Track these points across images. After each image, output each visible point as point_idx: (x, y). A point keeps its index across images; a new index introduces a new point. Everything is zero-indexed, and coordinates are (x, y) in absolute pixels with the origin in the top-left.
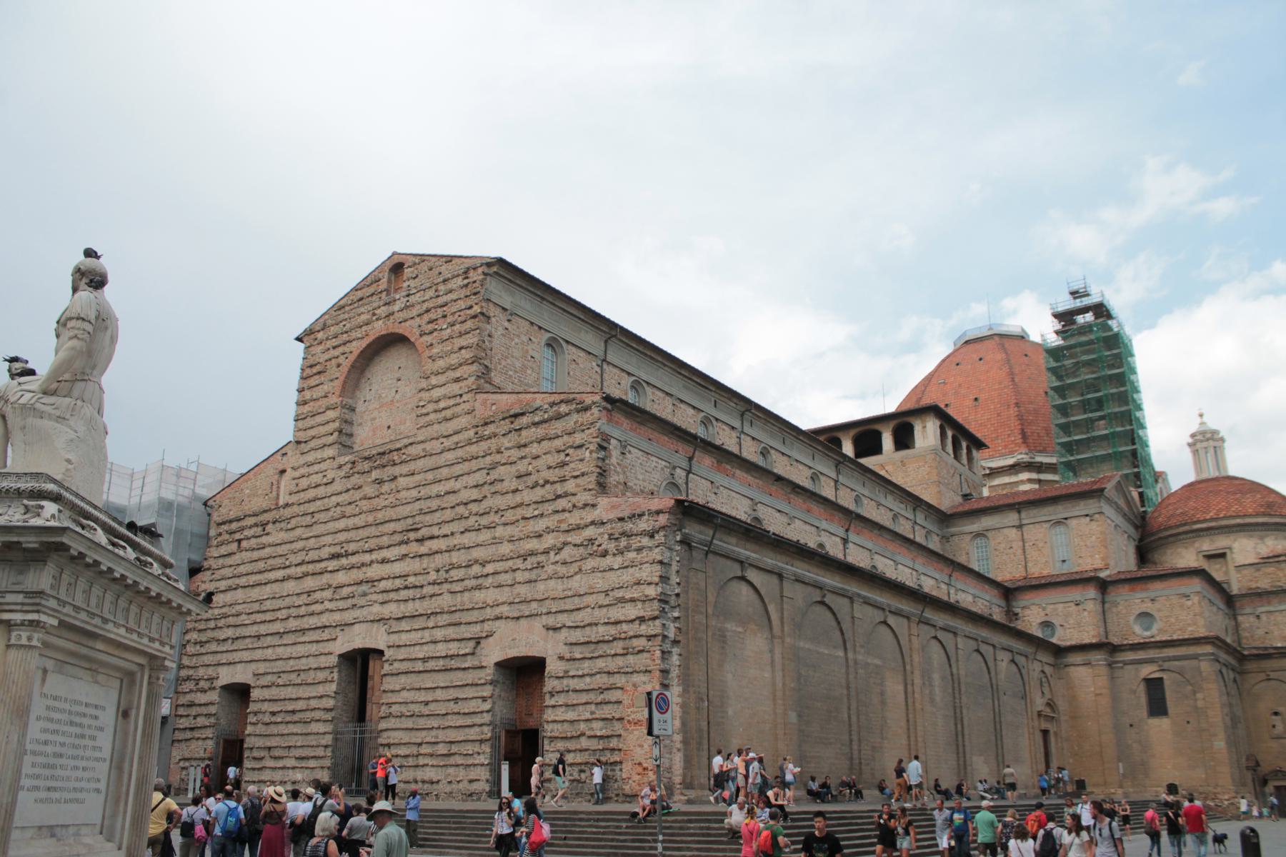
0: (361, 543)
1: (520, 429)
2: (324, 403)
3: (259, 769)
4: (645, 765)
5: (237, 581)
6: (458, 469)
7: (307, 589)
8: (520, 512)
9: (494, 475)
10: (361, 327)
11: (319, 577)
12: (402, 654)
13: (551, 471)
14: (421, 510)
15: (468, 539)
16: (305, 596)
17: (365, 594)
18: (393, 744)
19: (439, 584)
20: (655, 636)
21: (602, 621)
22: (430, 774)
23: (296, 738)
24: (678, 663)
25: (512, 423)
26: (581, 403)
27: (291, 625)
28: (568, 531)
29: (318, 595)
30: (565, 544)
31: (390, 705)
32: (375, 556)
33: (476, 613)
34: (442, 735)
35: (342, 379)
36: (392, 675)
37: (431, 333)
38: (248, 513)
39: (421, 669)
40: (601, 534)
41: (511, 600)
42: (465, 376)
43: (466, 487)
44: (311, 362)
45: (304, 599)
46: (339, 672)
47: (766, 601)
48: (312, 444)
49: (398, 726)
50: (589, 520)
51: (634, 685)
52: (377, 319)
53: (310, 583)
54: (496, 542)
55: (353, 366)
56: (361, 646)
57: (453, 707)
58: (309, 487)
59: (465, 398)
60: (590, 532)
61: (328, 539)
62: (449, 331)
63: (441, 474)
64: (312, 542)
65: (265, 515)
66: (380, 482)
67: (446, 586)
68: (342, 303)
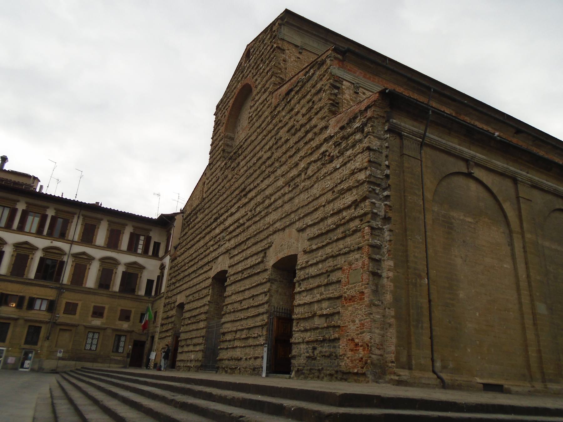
4: (357, 341)
9: (278, 137)
20: (365, 214)
22: (238, 353)
24: (388, 238)
30: (309, 164)
46: (213, 289)
47: (500, 199)
51: (350, 264)
54: (276, 180)
55: (230, 114)
57: (251, 302)
66: (233, 169)
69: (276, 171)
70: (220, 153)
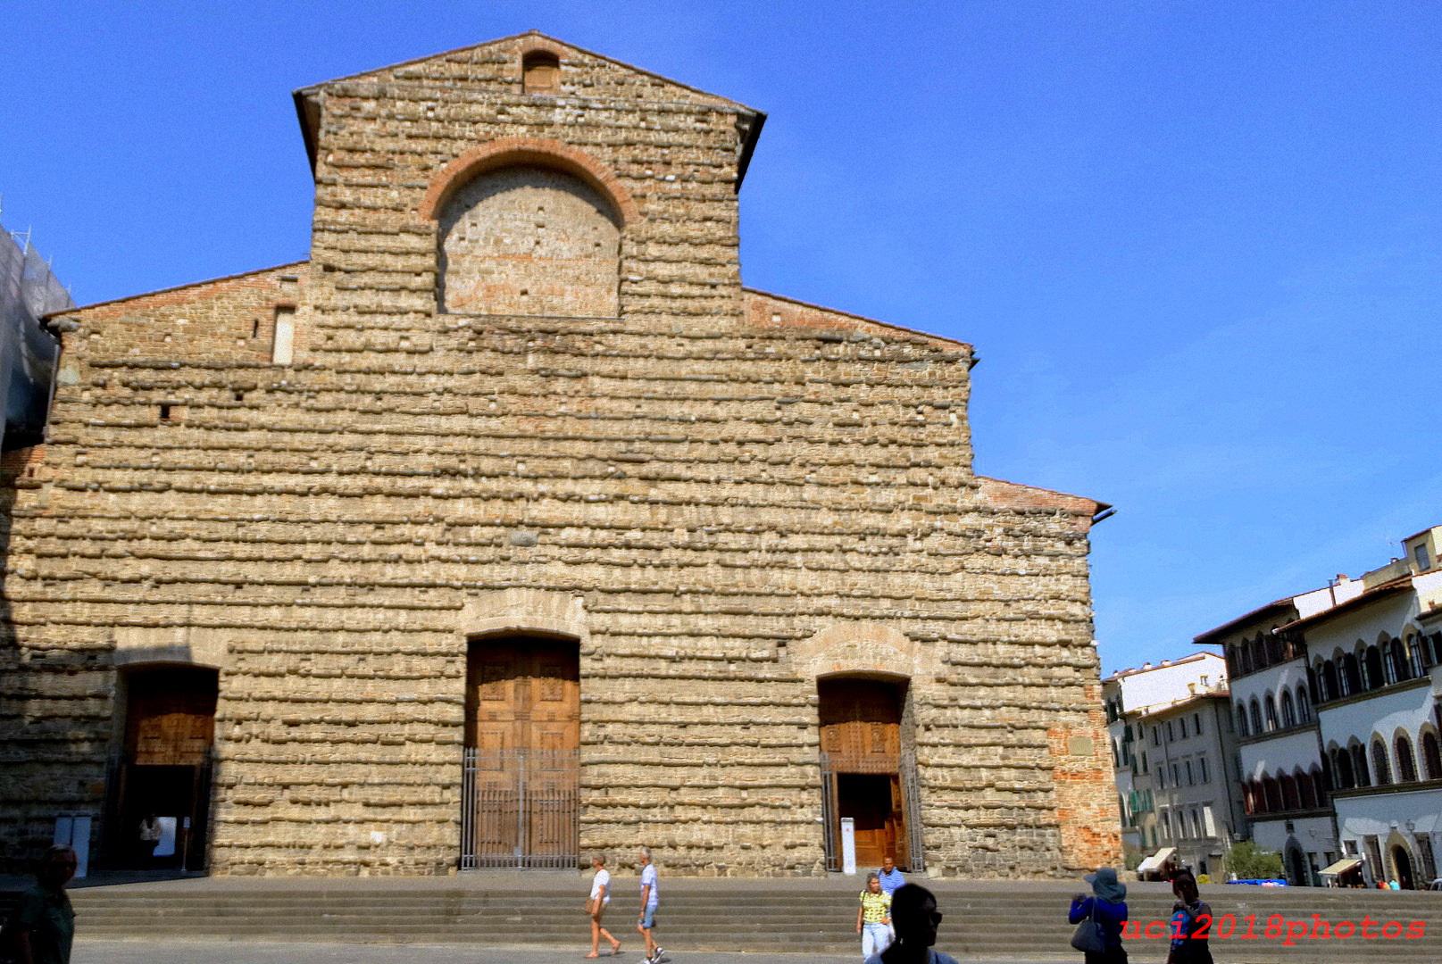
0: (506, 462)
1: (836, 360)
2: (393, 221)
3: (265, 823)
5: (163, 477)
6: (719, 390)
7: (379, 518)
8: (844, 474)
9: (793, 412)
10: (475, 123)
11: (405, 502)
12: (623, 645)
13: (896, 428)
14: (649, 434)
15: (746, 492)
16: (371, 527)
17: (528, 544)
18: (612, 787)
19: (695, 550)
21: (1006, 639)
23: (362, 768)
25: (818, 348)
26: (937, 351)
27: (332, 573)
28: (935, 513)
29: (406, 530)
30: (934, 530)
31: (601, 723)
32: (544, 487)
33: (775, 600)
34: (722, 776)
35: (439, 190)
36: (603, 677)
37: (642, 178)
38: (187, 360)
39: (672, 672)
40: (991, 527)
41: (846, 590)
42: (724, 261)
43: (738, 419)
44: (350, 144)
45: (368, 531)
48: (366, 279)
49: (629, 757)
50: (968, 504)
52: (514, 123)
53: (379, 507)
56: (524, 625)
58: (368, 347)
59: (722, 291)
60: (970, 520)
61: (428, 443)
62: (677, 186)
63: (683, 389)
64: (381, 441)
65: (241, 372)
66: (550, 375)
67: (711, 556)
68: (412, 68)
69: (801, 485)
70: (418, 274)
